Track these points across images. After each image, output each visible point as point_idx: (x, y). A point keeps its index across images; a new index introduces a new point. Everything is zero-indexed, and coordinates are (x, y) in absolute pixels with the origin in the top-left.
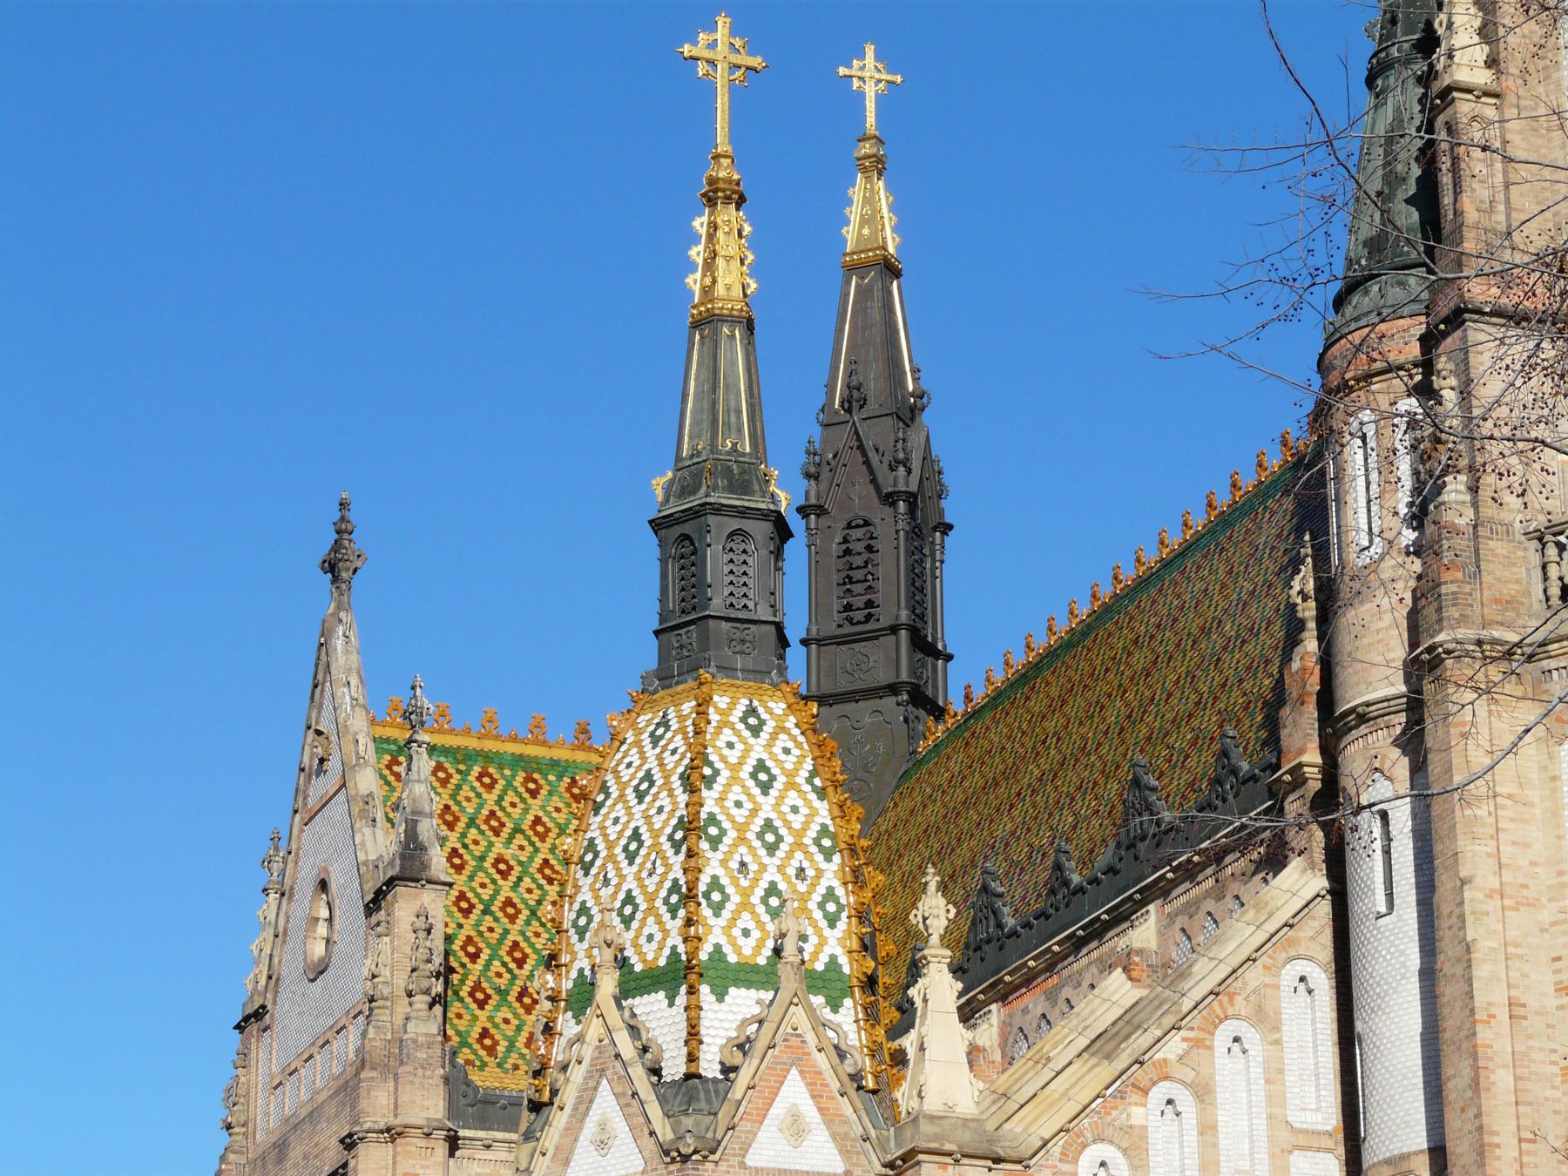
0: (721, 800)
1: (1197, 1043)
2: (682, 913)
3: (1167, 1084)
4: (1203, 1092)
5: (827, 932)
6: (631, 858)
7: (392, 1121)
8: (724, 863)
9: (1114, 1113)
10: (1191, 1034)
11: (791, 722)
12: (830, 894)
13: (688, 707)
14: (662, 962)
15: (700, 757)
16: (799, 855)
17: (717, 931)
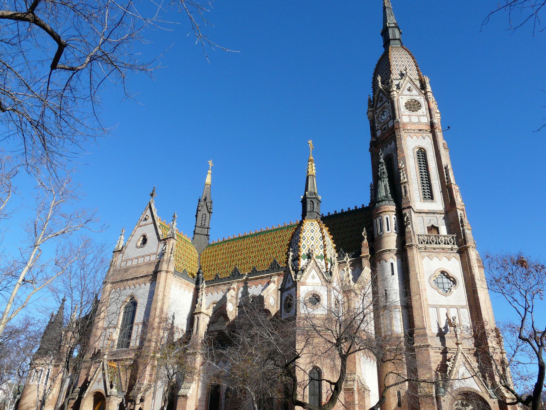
7: (167, 270)
14: (319, 255)
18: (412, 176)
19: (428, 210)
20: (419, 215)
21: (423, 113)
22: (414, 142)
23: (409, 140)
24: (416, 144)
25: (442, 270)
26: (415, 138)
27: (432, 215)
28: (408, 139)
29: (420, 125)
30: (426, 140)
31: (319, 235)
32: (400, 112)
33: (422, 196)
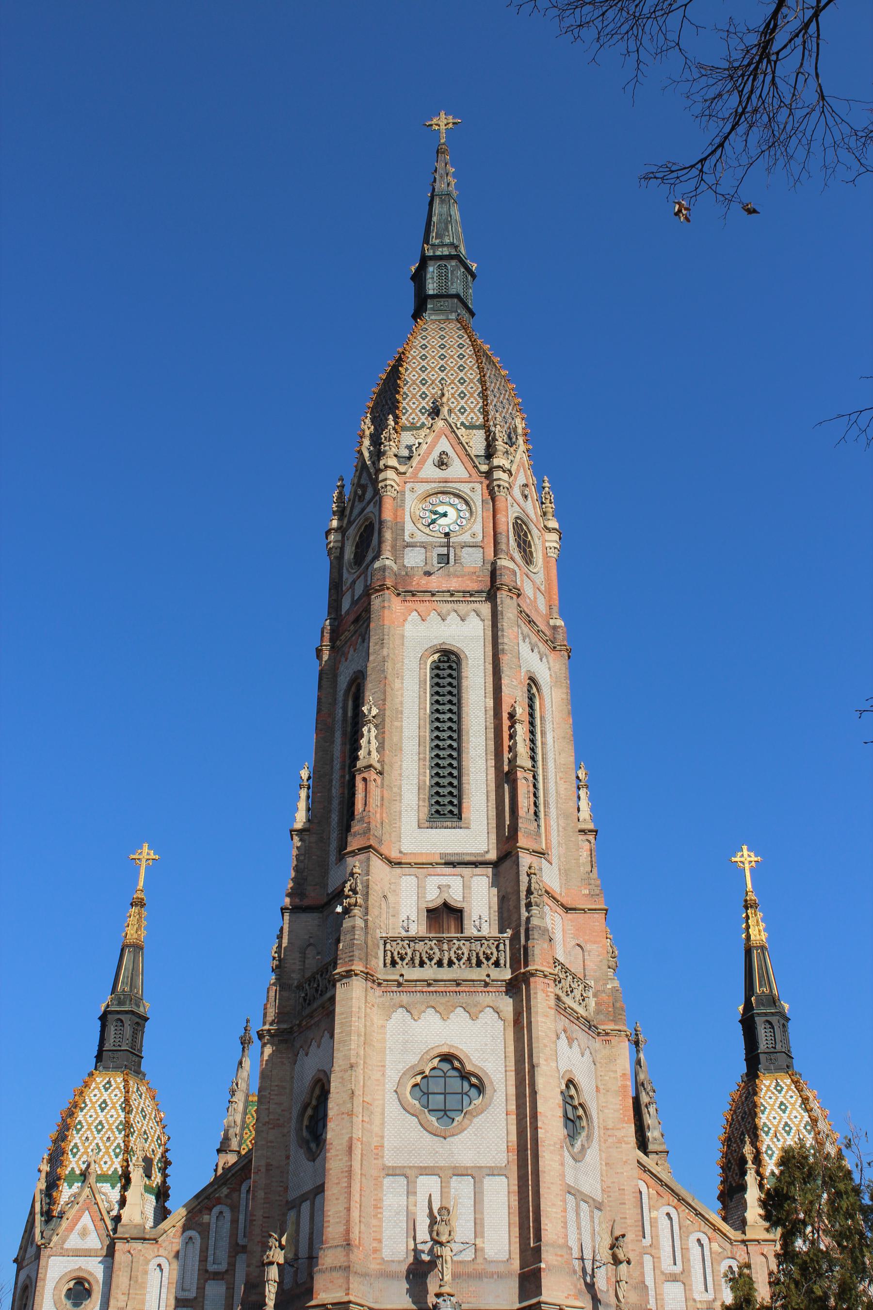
1: (233, 1190)
3: (220, 1206)
4: (235, 1209)
5: (115, 1160)
8: (80, 1138)
9: (196, 1219)
10: (231, 1186)
12: (118, 1146)
16: (109, 1133)
17: (73, 1163)
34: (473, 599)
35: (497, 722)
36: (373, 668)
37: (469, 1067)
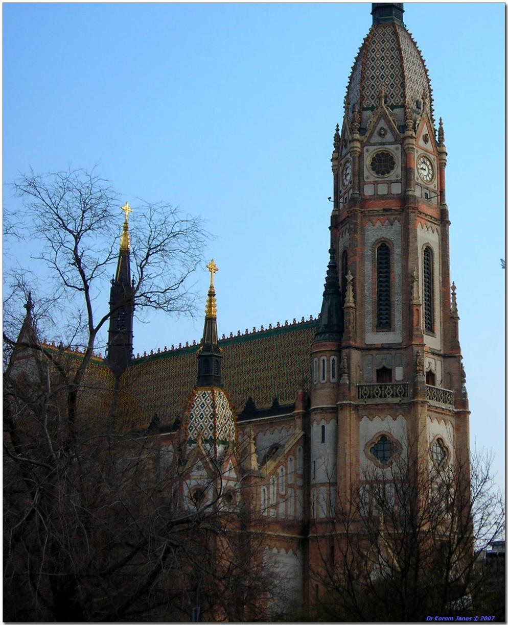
0: (218, 411)
2: (213, 430)
6: (201, 419)
11: (225, 396)
13: (209, 392)
15: (214, 403)
18: (366, 291)
19: (382, 344)
20: (368, 352)
21: (397, 176)
22: (376, 232)
23: (369, 228)
24: (378, 235)
25: (384, 433)
26: (378, 224)
27: (386, 352)
28: (369, 227)
29: (387, 201)
30: (393, 227)
31: (210, 412)
32: (361, 178)
33: (376, 323)
34: (436, 222)
35: (445, 290)
36: (412, 251)
37: (446, 445)
